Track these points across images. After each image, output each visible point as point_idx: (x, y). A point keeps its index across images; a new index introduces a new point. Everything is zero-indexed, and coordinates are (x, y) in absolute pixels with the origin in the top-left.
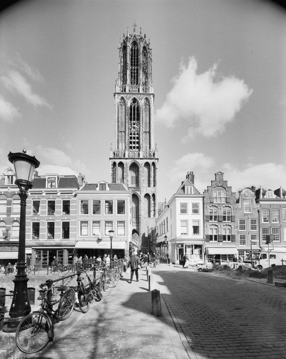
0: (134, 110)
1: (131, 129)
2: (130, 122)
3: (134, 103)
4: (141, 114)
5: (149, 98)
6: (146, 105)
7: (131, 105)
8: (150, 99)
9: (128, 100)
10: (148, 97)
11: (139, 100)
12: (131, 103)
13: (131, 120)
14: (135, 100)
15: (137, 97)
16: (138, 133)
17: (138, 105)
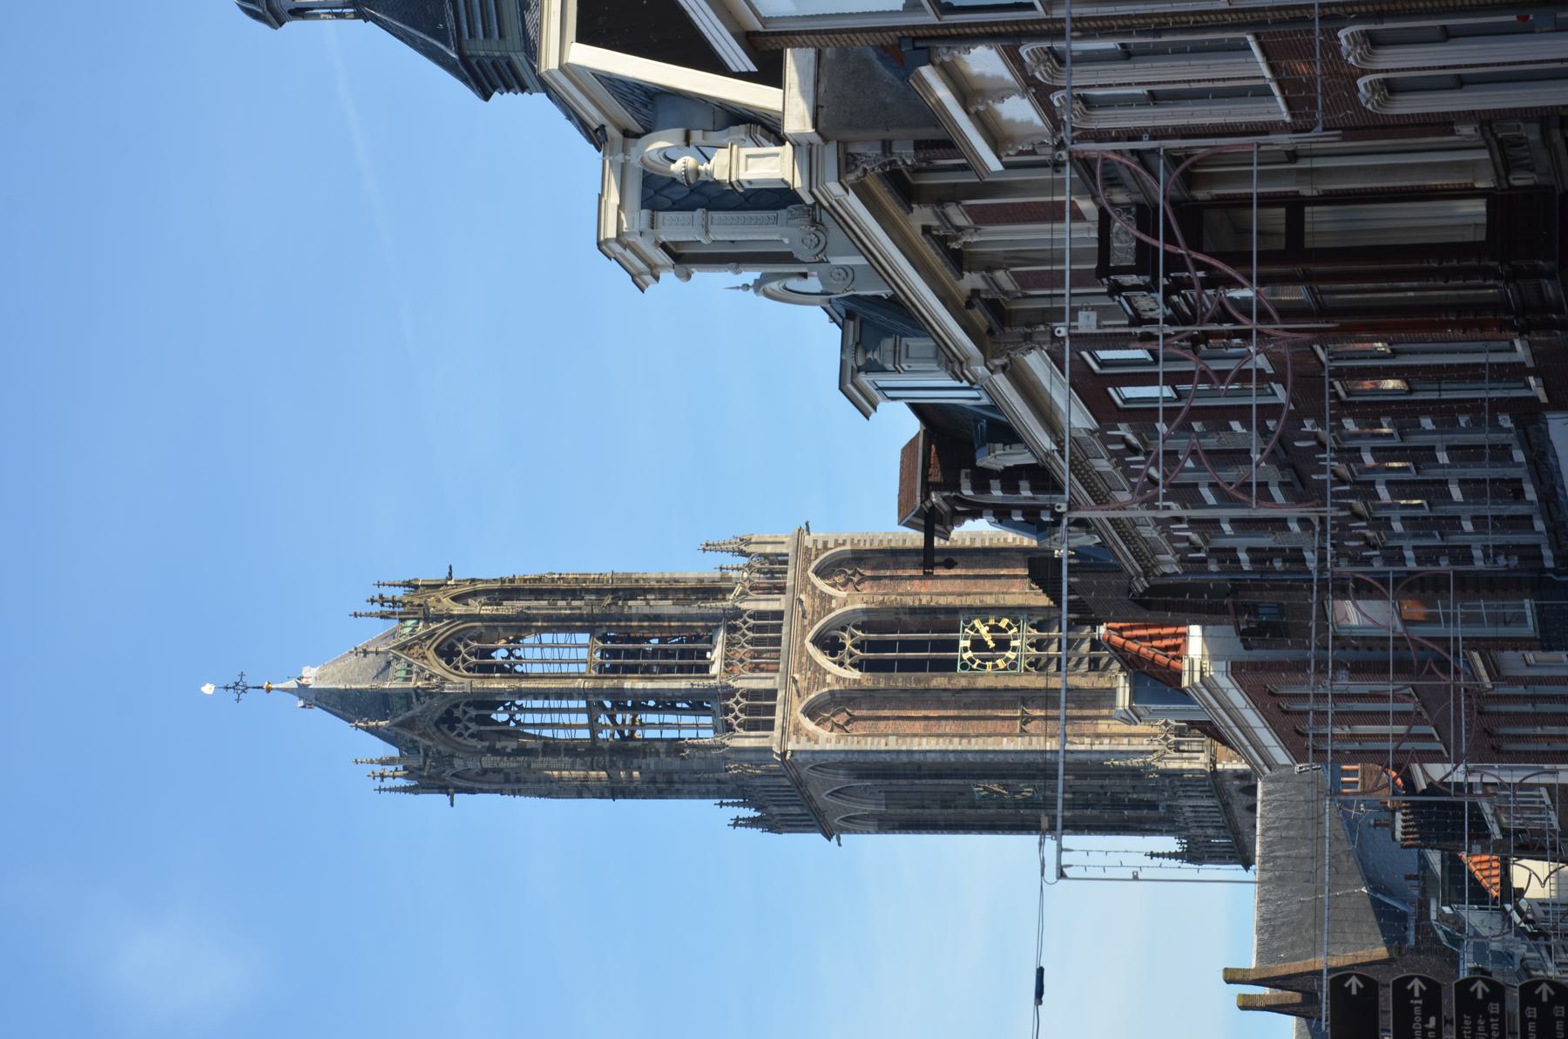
0: (889, 646)
1: (1007, 660)
2: (964, 666)
3: (843, 646)
4: (924, 602)
5: (821, 557)
6: (855, 579)
7: (854, 665)
8: (826, 548)
9: (829, 678)
10: (813, 565)
11: (831, 610)
12: (841, 664)
13: (948, 666)
14: (827, 643)
15: (812, 624)
16: (1033, 626)
17: (856, 627)
